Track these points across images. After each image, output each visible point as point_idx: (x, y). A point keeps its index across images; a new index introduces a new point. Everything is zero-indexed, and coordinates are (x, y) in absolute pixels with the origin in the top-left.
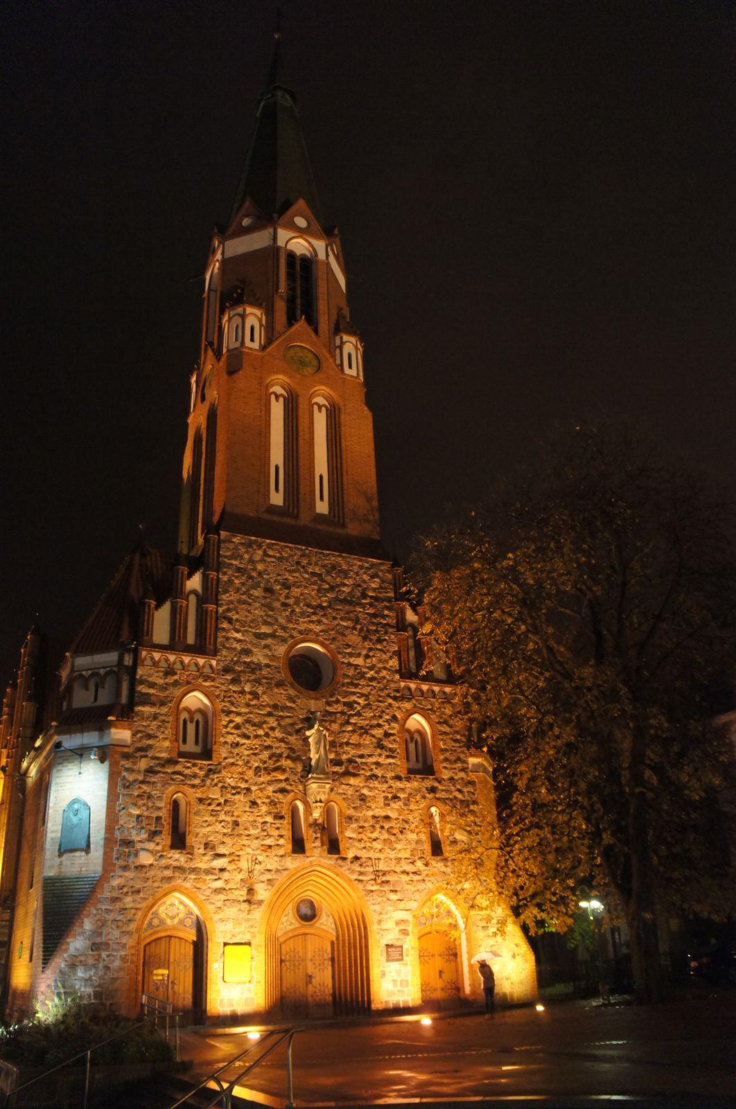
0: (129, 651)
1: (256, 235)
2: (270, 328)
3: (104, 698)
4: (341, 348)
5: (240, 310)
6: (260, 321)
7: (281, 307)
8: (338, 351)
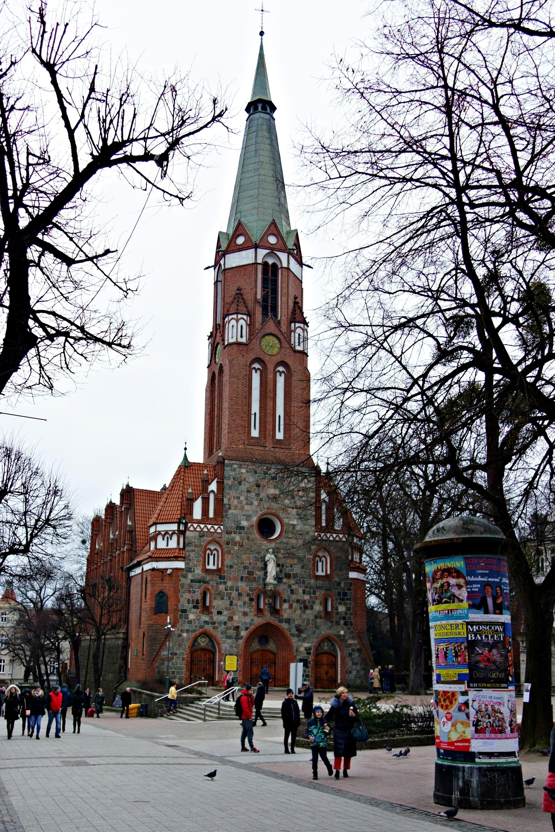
0: (182, 523)
1: (244, 253)
2: (250, 325)
3: (173, 544)
4: (294, 331)
5: (235, 316)
6: (246, 321)
7: (259, 311)
8: (293, 334)
